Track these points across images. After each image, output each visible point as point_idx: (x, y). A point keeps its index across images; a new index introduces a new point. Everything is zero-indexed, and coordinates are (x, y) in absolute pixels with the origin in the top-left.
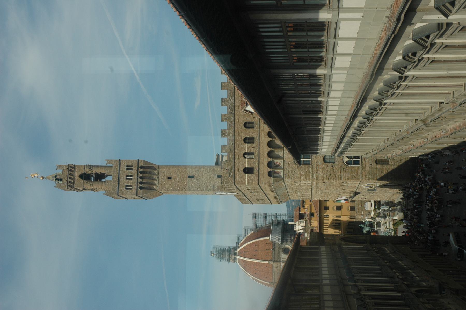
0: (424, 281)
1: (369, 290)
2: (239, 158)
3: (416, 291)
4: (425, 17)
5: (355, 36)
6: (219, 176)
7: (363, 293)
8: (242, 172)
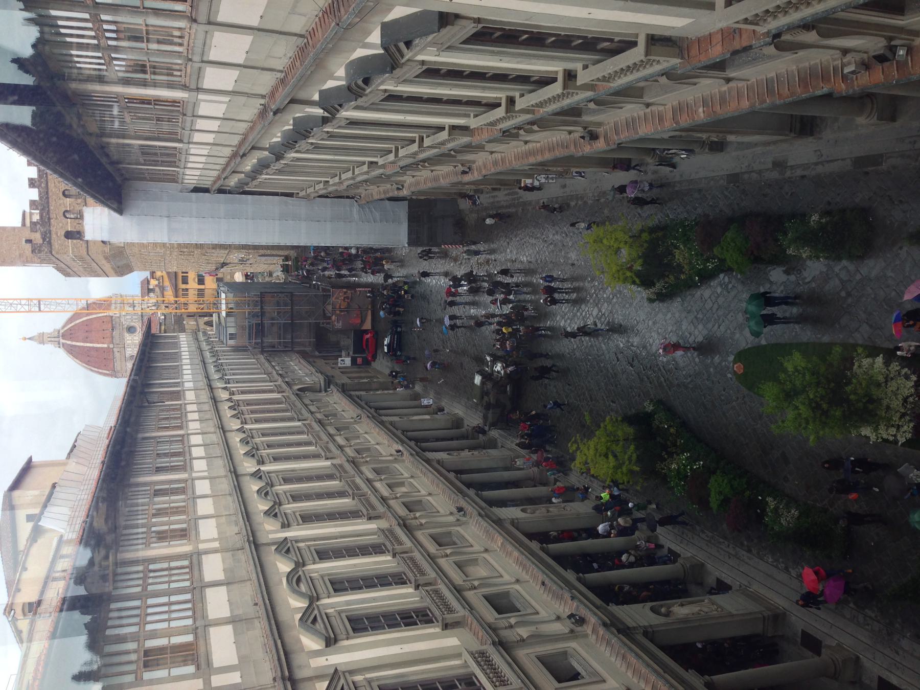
0: (307, 375)
1: (243, 392)
2: (56, 218)
3: (299, 390)
4: (307, 110)
5: (221, 116)
6: (29, 241)
7: (235, 397)
8: (63, 238)
